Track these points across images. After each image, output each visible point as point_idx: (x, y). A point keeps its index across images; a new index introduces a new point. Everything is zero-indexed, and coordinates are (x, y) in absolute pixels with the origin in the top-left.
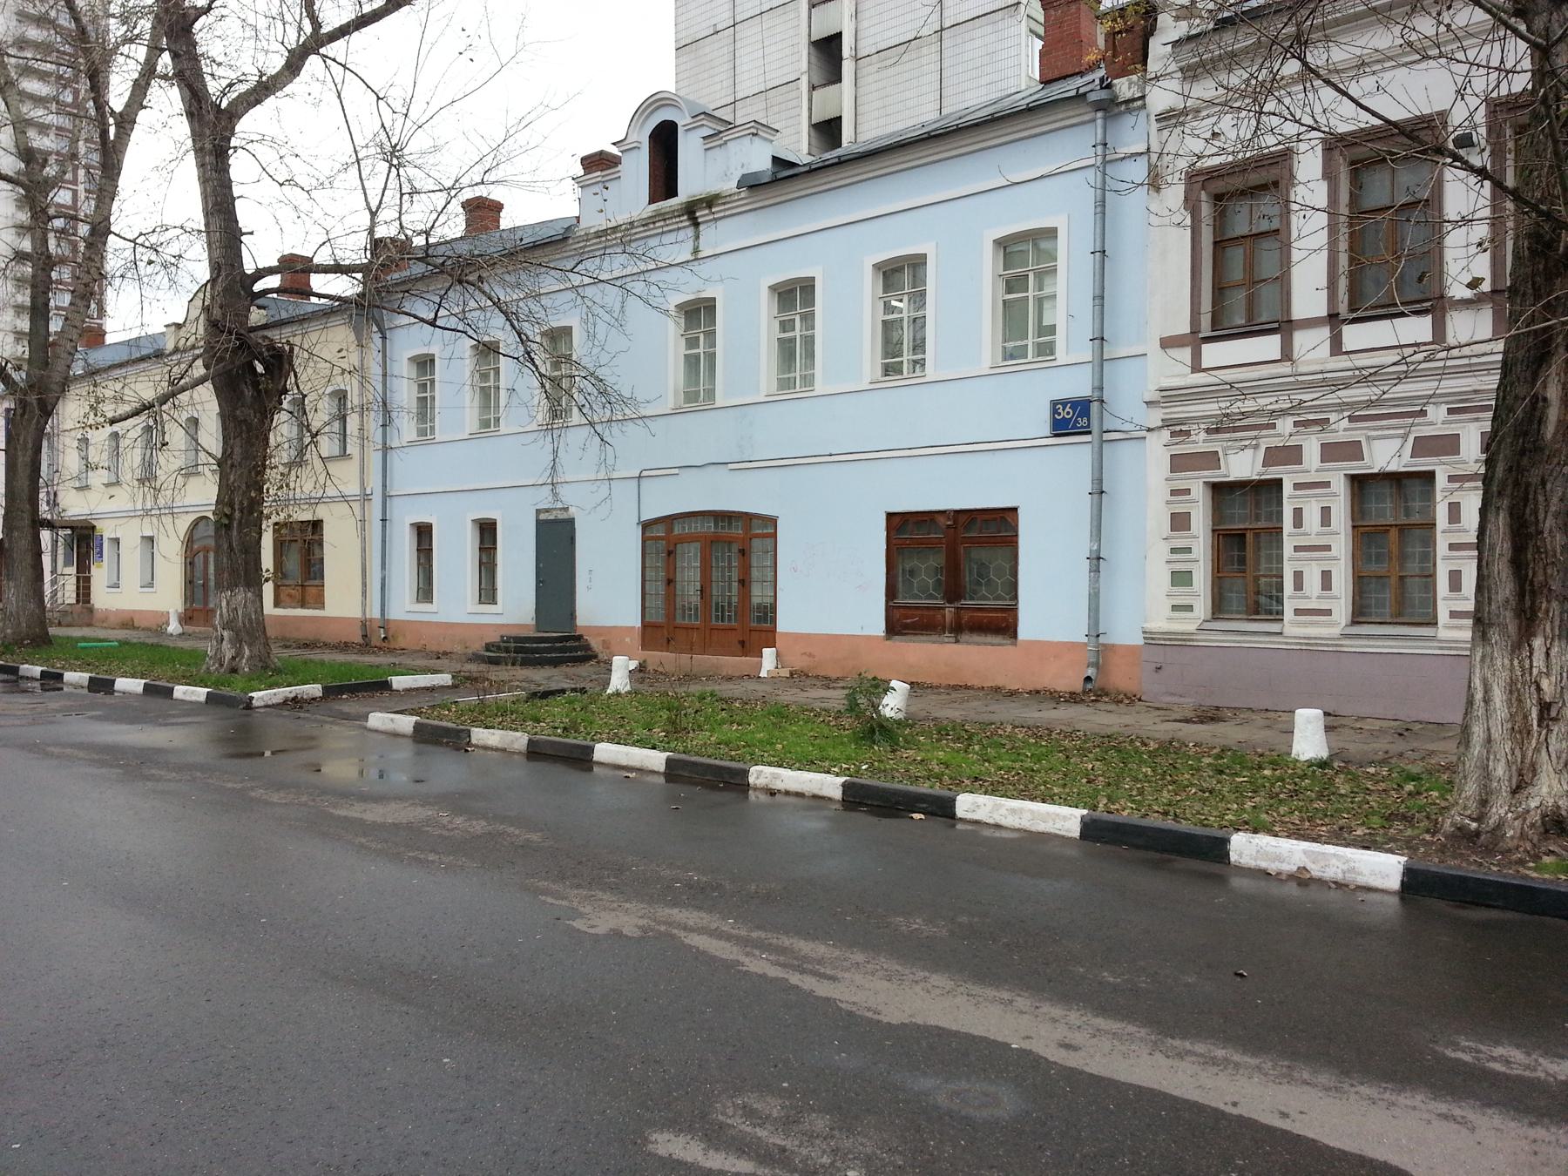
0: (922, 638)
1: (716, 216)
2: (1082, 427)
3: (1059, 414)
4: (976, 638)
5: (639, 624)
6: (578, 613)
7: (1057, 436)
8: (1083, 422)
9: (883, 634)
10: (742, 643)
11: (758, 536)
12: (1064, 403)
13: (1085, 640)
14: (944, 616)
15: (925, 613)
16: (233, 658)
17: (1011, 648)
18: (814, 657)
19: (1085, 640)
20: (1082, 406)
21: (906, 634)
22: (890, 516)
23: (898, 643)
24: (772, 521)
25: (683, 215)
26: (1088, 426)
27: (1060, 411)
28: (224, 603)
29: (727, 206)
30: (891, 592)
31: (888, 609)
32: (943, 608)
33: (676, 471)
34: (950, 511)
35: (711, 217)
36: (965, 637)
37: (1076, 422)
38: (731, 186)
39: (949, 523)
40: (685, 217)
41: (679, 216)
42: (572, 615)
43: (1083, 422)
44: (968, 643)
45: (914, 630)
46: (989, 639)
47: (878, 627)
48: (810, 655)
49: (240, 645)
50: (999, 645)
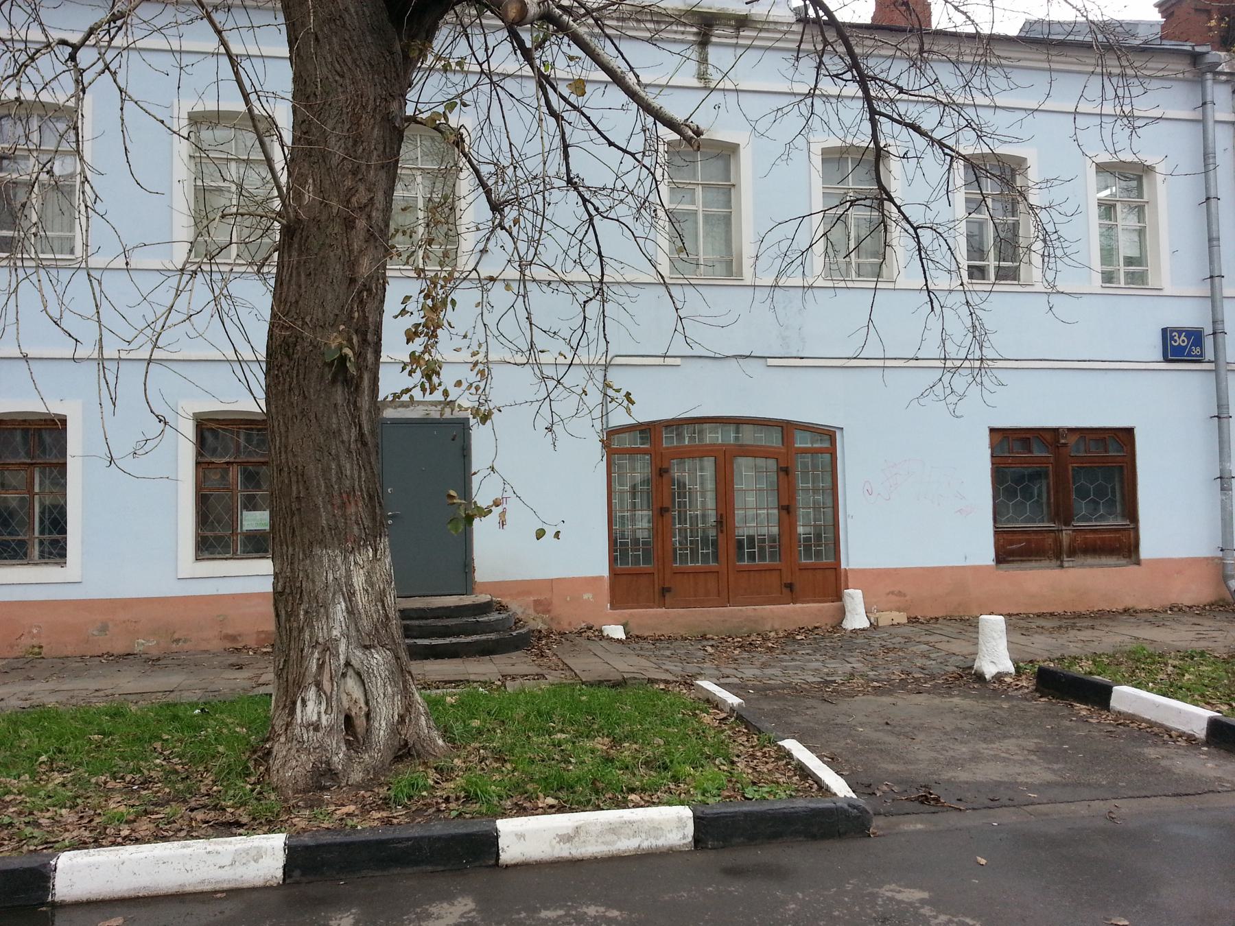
0: (1033, 564)
1: (741, 42)
2: (1196, 356)
3: (1175, 341)
4: (1090, 560)
5: (605, 572)
6: (476, 565)
7: (1166, 360)
8: (1196, 351)
9: (993, 563)
10: (790, 586)
11: (804, 451)
12: (1180, 331)
13: (1220, 554)
14: (1058, 542)
15: (1033, 537)
16: (402, 718)
17: (1136, 567)
18: (905, 595)
19: (1220, 554)
20: (1196, 336)
21: (1013, 561)
22: (992, 430)
23: (1011, 572)
24: (829, 435)
25: (692, 26)
26: (1201, 355)
27: (1176, 338)
28: (359, 580)
29: (763, 34)
30: (995, 520)
31: (997, 533)
32: (1062, 530)
33: (678, 361)
34: (1063, 429)
35: (734, 41)
36: (1080, 560)
37: (1191, 350)
38: (783, 14)
39: (1063, 441)
40: (695, 30)
41: (685, 24)
42: (467, 566)
43: (1196, 351)
44: (1082, 566)
45: (1020, 556)
46: (1104, 560)
47: (985, 553)
48: (900, 594)
49: (405, 682)
50: (1116, 566)
